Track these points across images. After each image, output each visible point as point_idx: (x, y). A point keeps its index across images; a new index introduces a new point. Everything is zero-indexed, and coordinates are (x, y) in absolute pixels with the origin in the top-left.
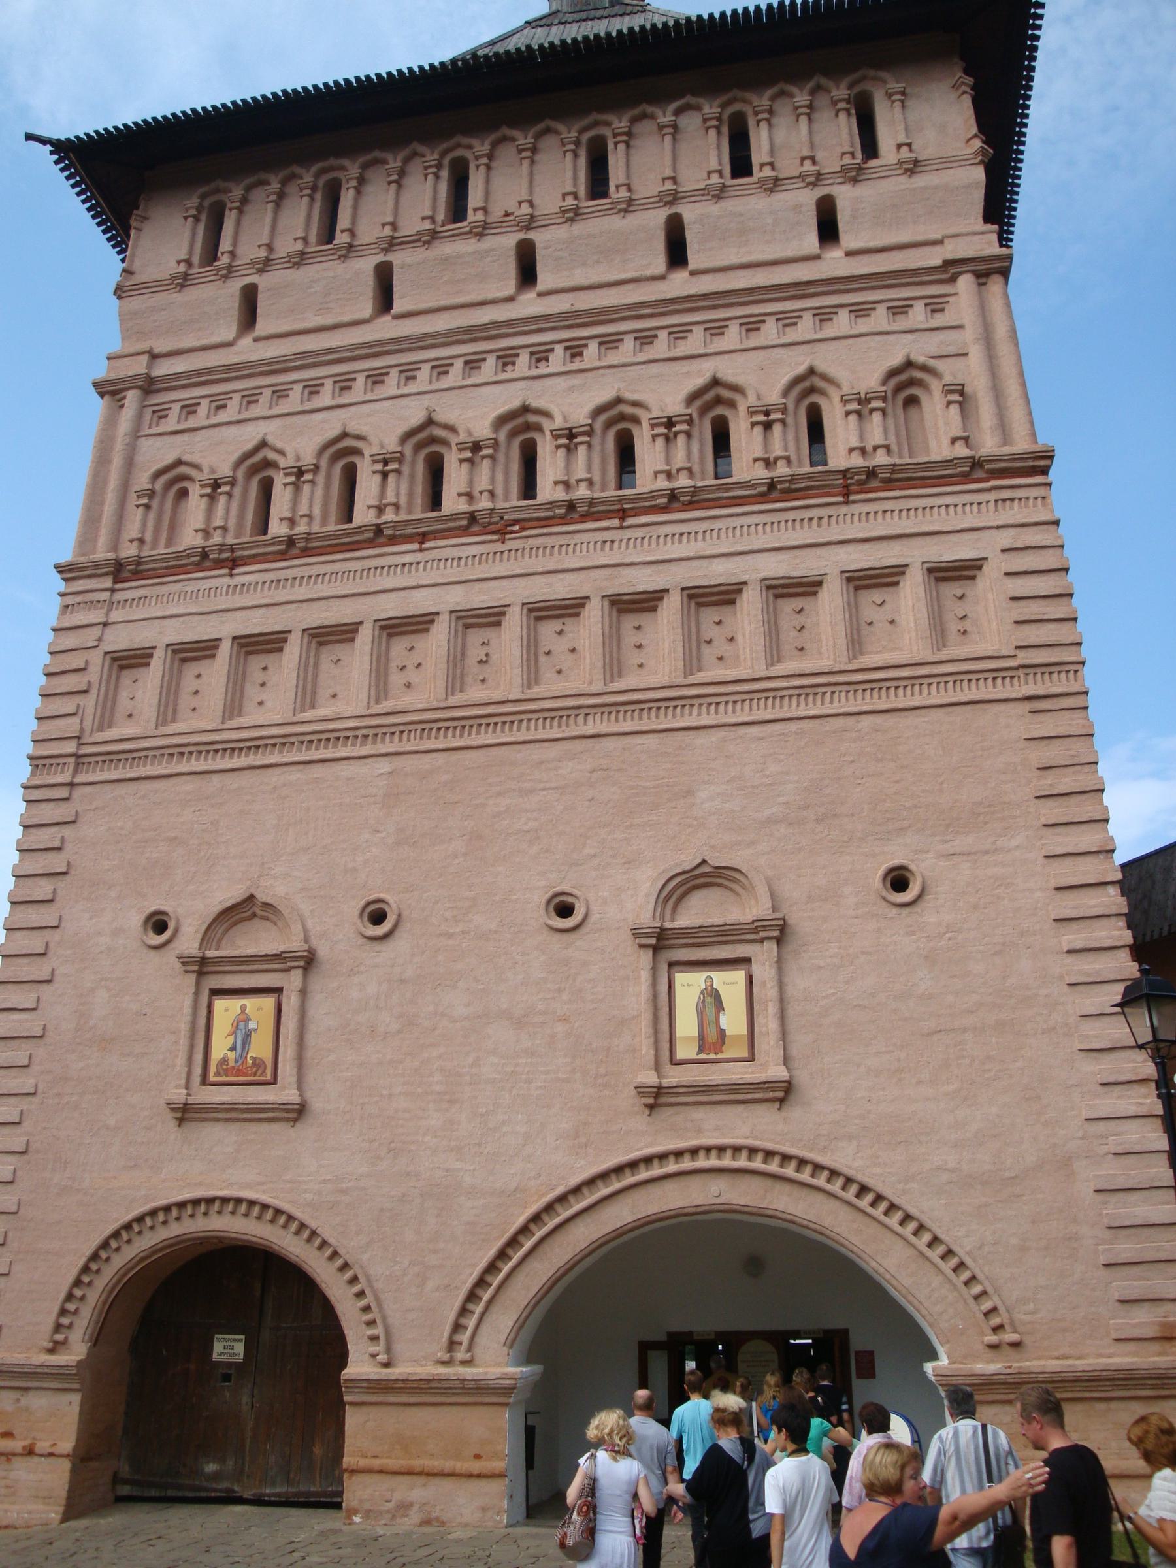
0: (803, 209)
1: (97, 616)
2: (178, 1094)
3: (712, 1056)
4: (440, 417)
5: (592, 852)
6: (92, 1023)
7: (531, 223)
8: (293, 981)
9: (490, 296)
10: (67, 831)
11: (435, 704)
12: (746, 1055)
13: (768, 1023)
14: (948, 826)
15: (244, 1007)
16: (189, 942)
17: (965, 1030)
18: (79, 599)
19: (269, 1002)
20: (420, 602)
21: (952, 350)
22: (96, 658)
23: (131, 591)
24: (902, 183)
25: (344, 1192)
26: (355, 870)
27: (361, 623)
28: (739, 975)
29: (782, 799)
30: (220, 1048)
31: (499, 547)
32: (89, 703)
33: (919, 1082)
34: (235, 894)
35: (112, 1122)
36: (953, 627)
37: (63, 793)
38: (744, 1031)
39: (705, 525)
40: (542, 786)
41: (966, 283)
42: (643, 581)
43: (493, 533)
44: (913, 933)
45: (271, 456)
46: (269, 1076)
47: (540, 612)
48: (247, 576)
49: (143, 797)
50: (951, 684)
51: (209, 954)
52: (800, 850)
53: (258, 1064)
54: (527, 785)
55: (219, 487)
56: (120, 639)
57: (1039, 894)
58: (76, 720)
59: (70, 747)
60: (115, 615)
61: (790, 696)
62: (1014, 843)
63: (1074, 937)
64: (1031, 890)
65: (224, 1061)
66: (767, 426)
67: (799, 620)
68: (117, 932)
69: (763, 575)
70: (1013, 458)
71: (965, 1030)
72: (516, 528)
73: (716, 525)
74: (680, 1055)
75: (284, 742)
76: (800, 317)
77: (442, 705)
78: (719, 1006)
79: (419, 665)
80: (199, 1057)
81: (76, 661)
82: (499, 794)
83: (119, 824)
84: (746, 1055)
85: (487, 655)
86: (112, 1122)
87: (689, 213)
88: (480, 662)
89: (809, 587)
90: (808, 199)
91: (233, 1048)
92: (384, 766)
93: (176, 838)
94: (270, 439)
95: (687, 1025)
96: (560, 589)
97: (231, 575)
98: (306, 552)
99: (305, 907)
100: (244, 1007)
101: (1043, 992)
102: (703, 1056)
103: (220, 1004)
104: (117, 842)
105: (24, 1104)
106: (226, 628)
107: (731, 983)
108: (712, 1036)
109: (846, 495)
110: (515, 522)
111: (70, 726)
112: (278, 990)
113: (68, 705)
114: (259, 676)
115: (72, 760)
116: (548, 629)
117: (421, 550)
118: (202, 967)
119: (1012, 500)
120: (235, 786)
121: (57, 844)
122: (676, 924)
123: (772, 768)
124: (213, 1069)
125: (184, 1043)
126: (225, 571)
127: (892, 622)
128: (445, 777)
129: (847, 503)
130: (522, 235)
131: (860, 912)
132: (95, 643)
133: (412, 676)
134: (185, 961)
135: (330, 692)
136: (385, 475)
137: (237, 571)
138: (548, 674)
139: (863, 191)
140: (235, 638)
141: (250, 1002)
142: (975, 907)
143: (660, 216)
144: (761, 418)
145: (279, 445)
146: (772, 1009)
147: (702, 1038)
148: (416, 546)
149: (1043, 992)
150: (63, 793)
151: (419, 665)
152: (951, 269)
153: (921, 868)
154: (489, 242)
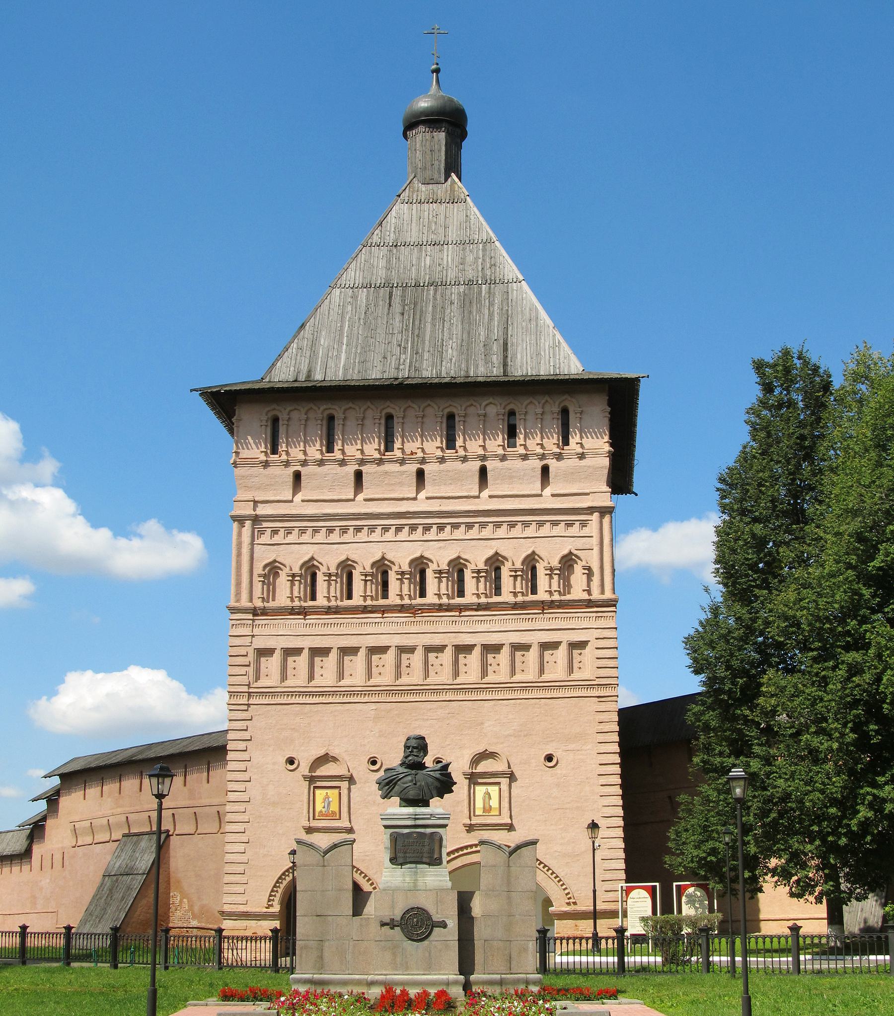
0: (536, 469)
1: (246, 631)
2: (306, 824)
3: (487, 814)
4: (387, 557)
5: (448, 743)
6: (268, 797)
7: (423, 461)
8: (344, 785)
9: (406, 496)
10: (248, 723)
11: (391, 684)
12: (498, 814)
13: (505, 804)
14: (567, 741)
15: (327, 793)
16: (304, 769)
17: (566, 809)
18: (238, 622)
19: (336, 791)
20: (382, 641)
21: (587, 547)
22: (251, 651)
23: (261, 620)
24: (575, 462)
25: (367, 856)
26: (364, 745)
27: (361, 647)
28: (496, 788)
29: (513, 728)
30: (319, 807)
31: (412, 619)
32: (251, 670)
33: (552, 825)
34: (322, 752)
35: (281, 832)
36: (576, 665)
37: (245, 707)
38: (497, 806)
39: (491, 618)
40: (430, 718)
41: (596, 515)
42: (467, 640)
43: (410, 613)
44: (552, 776)
45: (316, 563)
46: (338, 817)
47: (429, 649)
48: (312, 619)
49: (279, 711)
50: (572, 689)
51: (313, 774)
52: (518, 746)
53: (334, 813)
54: (426, 717)
55: (295, 576)
56: (260, 643)
57: (594, 766)
58: (246, 677)
59: (245, 689)
60: (256, 631)
61: (518, 690)
62: (588, 748)
63: (603, 780)
64: (591, 764)
65: (321, 812)
66: (515, 577)
67: (523, 659)
68: (274, 764)
69: (511, 642)
70: (604, 601)
71: (566, 809)
72: (420, 612)
73: (495, 618)
74: (477, 813)
75: (334, 693)
76: (531, 524)
77: (394, 684)
78: (490, 798)
79: (384, 666)
80: (311, 810)
81: (243, 651)
82: (416, 720)
83: (271, 721)
84: (498, 814)
85: (409, 664)
86: (281, 832)
87: (489, 464)
88: (407, 667)
89: (526, 647)
90: (538, 464)
91: (324, 807)
92: (373, 706)
93: (294, 729)
94: (315, 557)
95: (479, 804)
96: (436, 640)
97: (305, 619)
98: (336, 613)
99: (347, 758)
100: (327, 793)
101: (592, 797)
102: (484, 814)
103: (318, 792)
104: (270, 729)
105: (245, 825)
106: (306, 643)
107: (494, 790)
108: (487, 806)
109: (543, 611)
110: (420, 609)
111: (244, 680)
112: (339, 787)
113: (243, 670)
114: (321, 664)
115: (247, 694)
116: (432, 656)
117: (383, 618)
118: (311, 780)
119: (602, 617)
120: (316, 710)
121: (246, 728)
122: (476, 771)
123: (511, 716)
124: (317, 814)
125: (306, 805)
126: (302, 617)
127: (555, 662)
128: (396, 712)
129: (543, 613)
130: (419, 466)
131: (536, 769)
132: (250, 644)
133: (381, 669)
134: (305, 777)
135: (350, 673)
136: (366, 581)
137: (307, 617)
138: (431, 673)
139: (561, 464)
140: (310, 648)
141: (329, 791)
142: (573, 769)
143: (478, 464)
144: (513, 574)
145: (320, 560)
146: (507, 800)
147: (484, 808)
148: (380, 615)
149: (592, 797)
150: (245, 707)
151: (384, 666)
152: (591, 510)
153: (557, 755)
154: (405, 468)
